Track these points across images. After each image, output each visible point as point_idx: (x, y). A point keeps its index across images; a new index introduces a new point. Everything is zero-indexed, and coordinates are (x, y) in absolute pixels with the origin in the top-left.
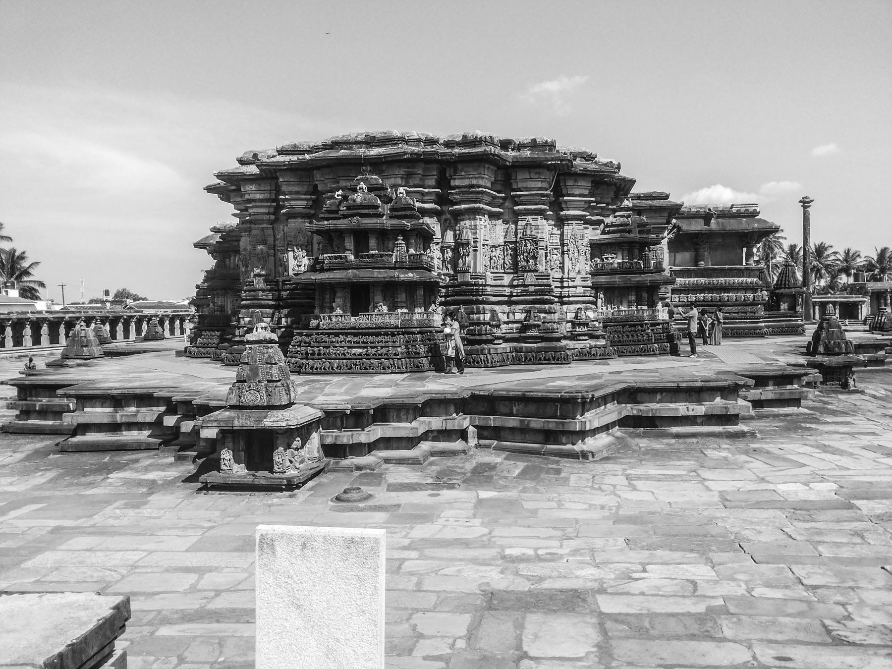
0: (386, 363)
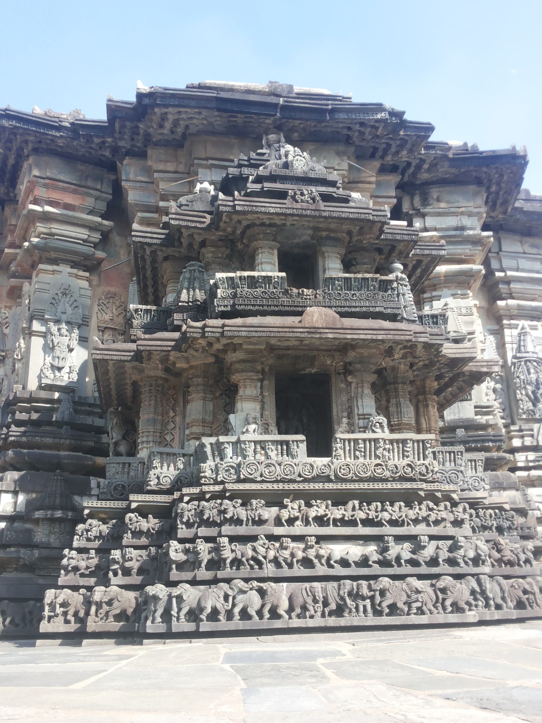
0: (462, 591)
